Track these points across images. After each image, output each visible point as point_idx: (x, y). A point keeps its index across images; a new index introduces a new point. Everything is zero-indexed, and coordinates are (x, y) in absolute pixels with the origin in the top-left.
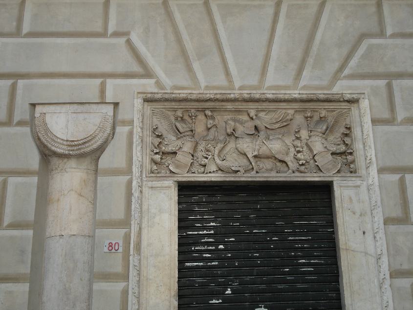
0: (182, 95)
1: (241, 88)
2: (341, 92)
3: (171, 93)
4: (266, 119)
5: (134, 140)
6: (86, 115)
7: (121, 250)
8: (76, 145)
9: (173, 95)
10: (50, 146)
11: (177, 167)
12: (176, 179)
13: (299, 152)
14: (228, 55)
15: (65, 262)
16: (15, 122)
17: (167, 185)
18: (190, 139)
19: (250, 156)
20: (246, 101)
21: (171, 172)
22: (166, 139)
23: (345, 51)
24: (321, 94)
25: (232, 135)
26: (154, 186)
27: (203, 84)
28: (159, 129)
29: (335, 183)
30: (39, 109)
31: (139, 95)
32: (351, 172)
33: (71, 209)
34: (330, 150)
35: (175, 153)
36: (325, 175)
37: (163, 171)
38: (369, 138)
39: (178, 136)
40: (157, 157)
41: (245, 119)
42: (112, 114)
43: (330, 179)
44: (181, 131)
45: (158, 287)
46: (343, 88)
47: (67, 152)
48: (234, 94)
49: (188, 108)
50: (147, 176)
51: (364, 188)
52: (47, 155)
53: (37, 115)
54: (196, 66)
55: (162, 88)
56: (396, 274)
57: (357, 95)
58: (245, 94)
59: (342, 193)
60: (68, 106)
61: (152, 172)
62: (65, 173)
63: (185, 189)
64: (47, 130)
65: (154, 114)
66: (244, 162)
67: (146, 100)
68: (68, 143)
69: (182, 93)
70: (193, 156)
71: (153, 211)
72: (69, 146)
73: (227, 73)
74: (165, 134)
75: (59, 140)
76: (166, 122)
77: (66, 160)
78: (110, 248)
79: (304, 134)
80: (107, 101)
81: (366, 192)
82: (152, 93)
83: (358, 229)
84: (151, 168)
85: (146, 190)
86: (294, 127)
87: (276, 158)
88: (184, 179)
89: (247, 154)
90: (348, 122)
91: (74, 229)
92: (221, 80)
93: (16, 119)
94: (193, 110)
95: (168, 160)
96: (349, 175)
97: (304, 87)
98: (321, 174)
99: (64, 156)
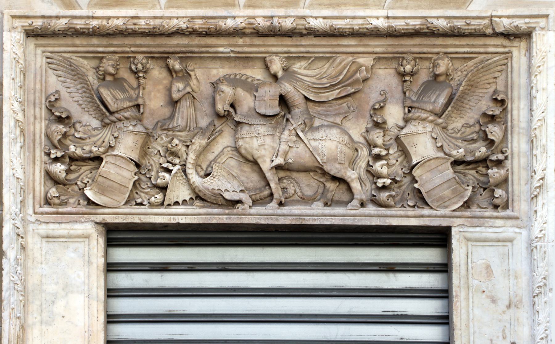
0: (119, 23)
2: (488, 14)
3: (88, 17)
11: (102, 191)
12: (99, 219)
13: (378, 157)
17: (80, 232)
18: (131, 128)
19: (266, 166)
21: (90, 202)
22: (78, 126)
26: (51, 233)
28: (63, 104)
29: (454, 231)
31: (18, 23)
32: (496, 207)
34: (449, 155)
35: (98, 159)
36: (434, 212)
37: (72, 201)
38: (544, 127)
39: (107, 121)
40: (59, 169)
41: (259, 77)
43: (444, 223)
44: (112, 109)
48: (234, 17)
49: (127, 52)
51: (520, 245)
57: (527, 20)
61: (48, 202)
65: (52, 66)
69: (114, 17)
70: (138, 165)
74: (76, 112)
76: (79, 87)
81: (524, 253)
83: (501, 338)
84: (46, 193)
87: (324, 173)
89: (259, 161)
90: (501, 88)
96: (490, 212)
98: (426, 211)
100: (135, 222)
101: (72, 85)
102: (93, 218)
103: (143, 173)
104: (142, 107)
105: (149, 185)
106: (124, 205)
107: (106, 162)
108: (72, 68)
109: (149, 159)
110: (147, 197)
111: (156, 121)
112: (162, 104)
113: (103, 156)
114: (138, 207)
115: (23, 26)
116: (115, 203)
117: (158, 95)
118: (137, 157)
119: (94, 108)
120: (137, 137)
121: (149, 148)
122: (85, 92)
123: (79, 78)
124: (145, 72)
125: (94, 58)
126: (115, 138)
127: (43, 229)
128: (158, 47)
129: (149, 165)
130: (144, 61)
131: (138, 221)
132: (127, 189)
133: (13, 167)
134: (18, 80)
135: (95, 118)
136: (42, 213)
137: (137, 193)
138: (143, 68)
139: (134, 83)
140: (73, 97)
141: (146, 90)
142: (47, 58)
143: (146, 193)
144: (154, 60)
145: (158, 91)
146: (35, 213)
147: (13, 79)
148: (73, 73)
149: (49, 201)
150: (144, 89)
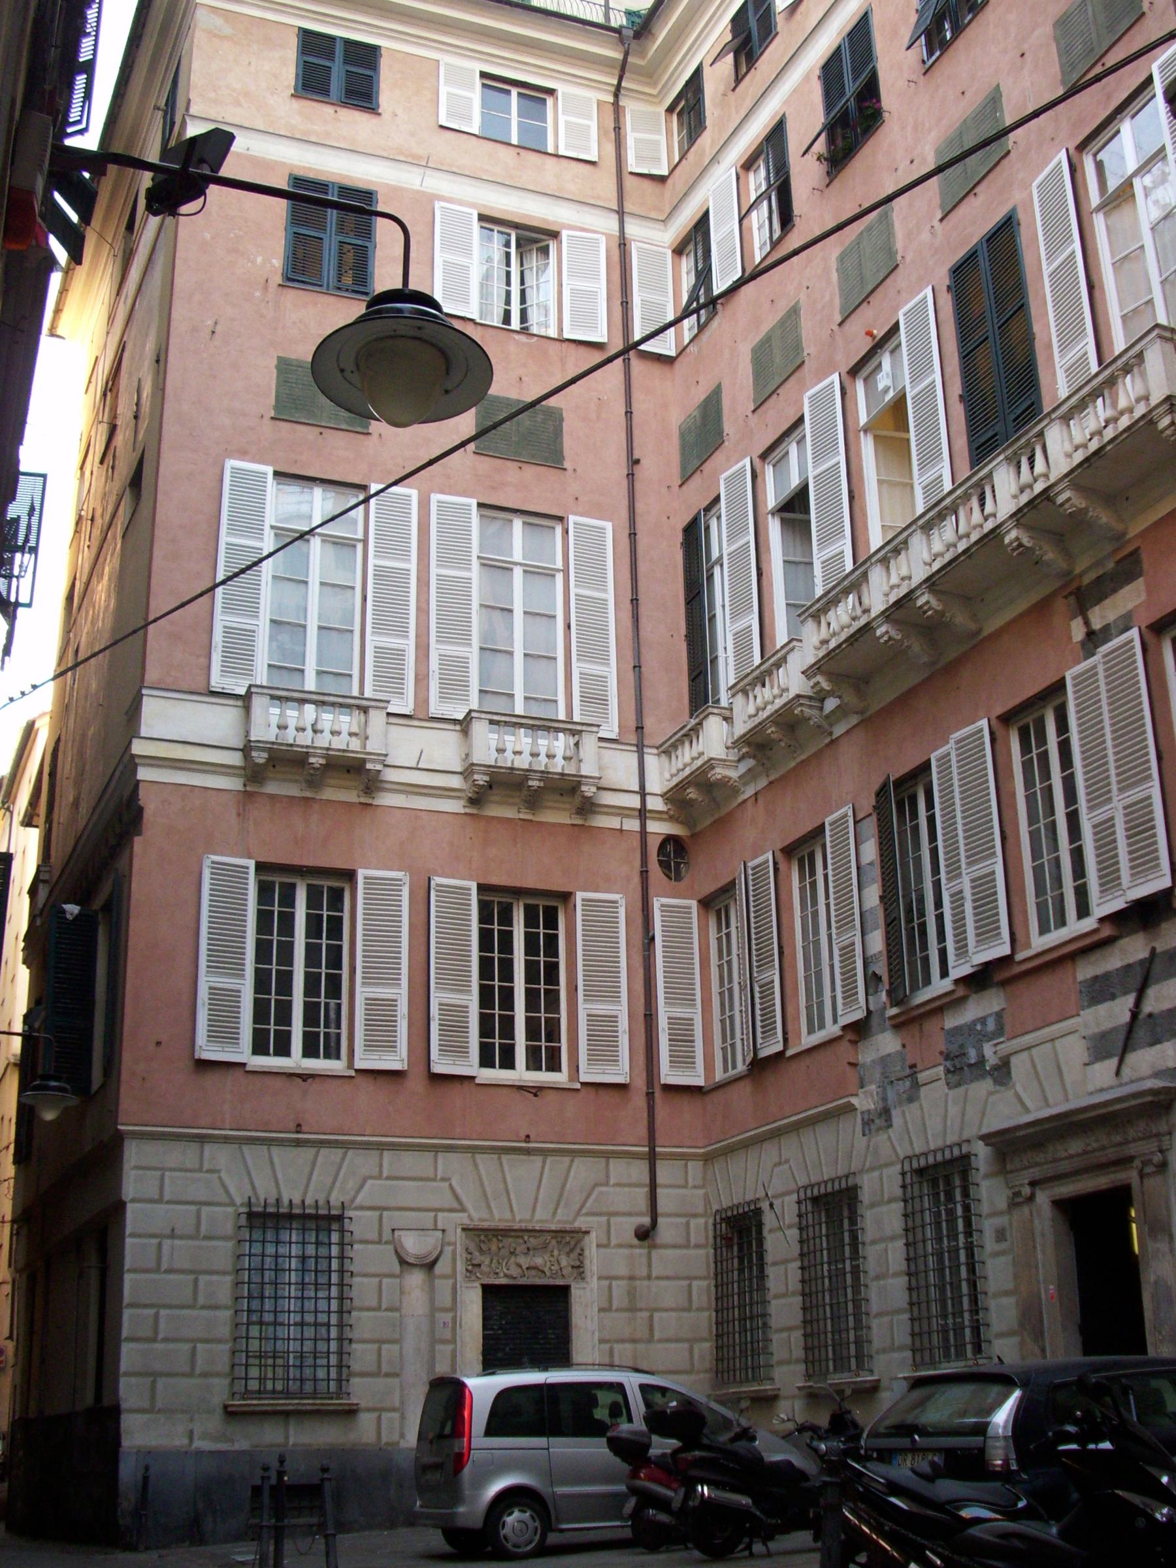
1: (521, 1221)
4: (533, 1242)
14: (512, 1197)
19: (524, 1268)
20: (522, 1230)
23: (584, 1195)
24: (568, 1227)
25: (512, 1253)
27: (497, 1217)
30: (396, 1233)
40: (470, 1268)
46: (581, 1223)
52: (403, 1262)
54: (493, 1205)
55: (471, 1219)
56: (601, 1341)
58: (523, 1225)
59: (575, 1293)
63: (487, 1289)
64: (402, 1247)
66: (519, 1271)
67: (463, 1229)
73: (512, 1210)
79: (556, 1253)
86: (550, 1248)
91: (421, 1312)
92: (508, 1216)
93: (384, 1240)
95: (476, 1270)
97: (559, 1222)
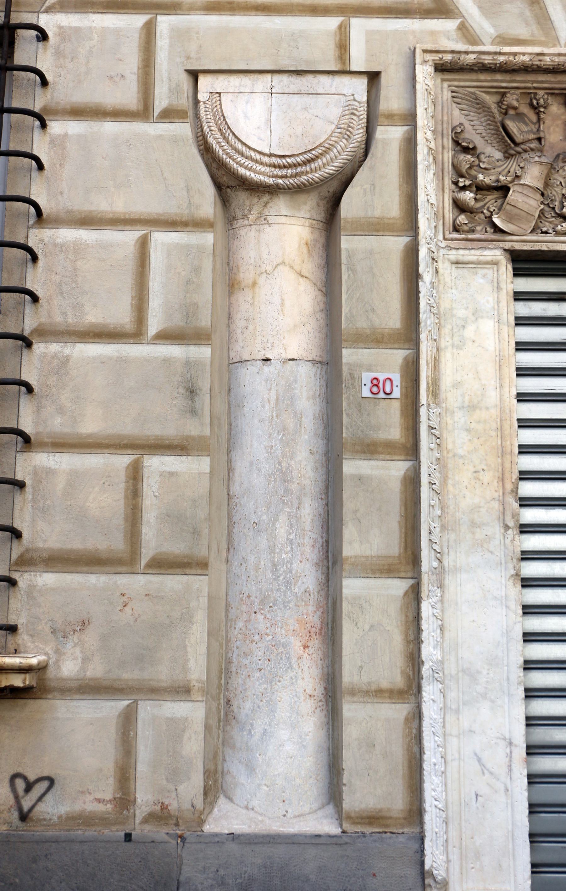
3: (496, 53)
5: (420, 158)
6: (307, 100)
7: (397, 393)
8: (290, 166)
9: (502, 58)
10: (235, 165)
11: (510, 219)
12: (508, 246)
15: (277, 416)
16: (157, 111)
17: (489, 258)
18: (537, 159)
21: (497, 230)
22: (482, 157)
26: (461, 258)
28: (466, 135)
30: (203, 81)
31: (429, 57)
33: (282, 304)
35: (504, 190)
37: (479, 228)
39: (512, 152)
40: (468, 196)
42: (365, 99)
45: (475, 472)
47: (271, 181)
49: (529, 88)
50: (448, 236)
53: (202, 97)
60: (269, 76)
62: (266, 226)
68: (274, 160)
69: (520, 54)
70: (543, 195)
71: (461, 313)
72: (275, 166)
75: (253, 154)
76: (483, 119)
77: (266, 198)
78: (375, 390)
80: (354, 68)
82: (453, 52)
84: (454, 221)
85: (444, 267)
88: (527, 247)
94: (541, 93)
99: (261, 189)
100: (542, 249)
101: (475, 118)
102: (501, 244)
103: (546, 203)
104: (543, 140)
105: (553, 215)
106: (531, 232)
107: (514, 191)
108: (478, 101)
109: (551, 190)
110: (552, 226)
111: (556, 154)
112: (561, 138)
113: (510, 185)
114: (544, 235)
115: (433, 60)
116: (522, 231)
117: (557, 129)
118: (542, 186)
119: (498, 140)
120: (543, 168)
121: (550, 179)
122: (489, 125)
123: (484, 111)
124: (545, 108)
125: (497, 93)
126: (521, 168)
127: (453, 255)
128: (559, 84)
129: (551, 195)
130: (546, 96)
131: (546, 249)
132: (533, 217)
133: (427, 193)
134: (430, 110)
135: (498, 149)
136: (452, 240)
137: (541, 222)
138: (544, 103)
139: (534, 118)
140: (476, 130)
141: (546, 124)
142: (452, 92)
143: (550, 222)
144: (554, 96)
145: (557, 126)
146: (445, 239)
147: (426, 109)
148: (478, 106)
149: (458, 227)
150: (544, 123)
